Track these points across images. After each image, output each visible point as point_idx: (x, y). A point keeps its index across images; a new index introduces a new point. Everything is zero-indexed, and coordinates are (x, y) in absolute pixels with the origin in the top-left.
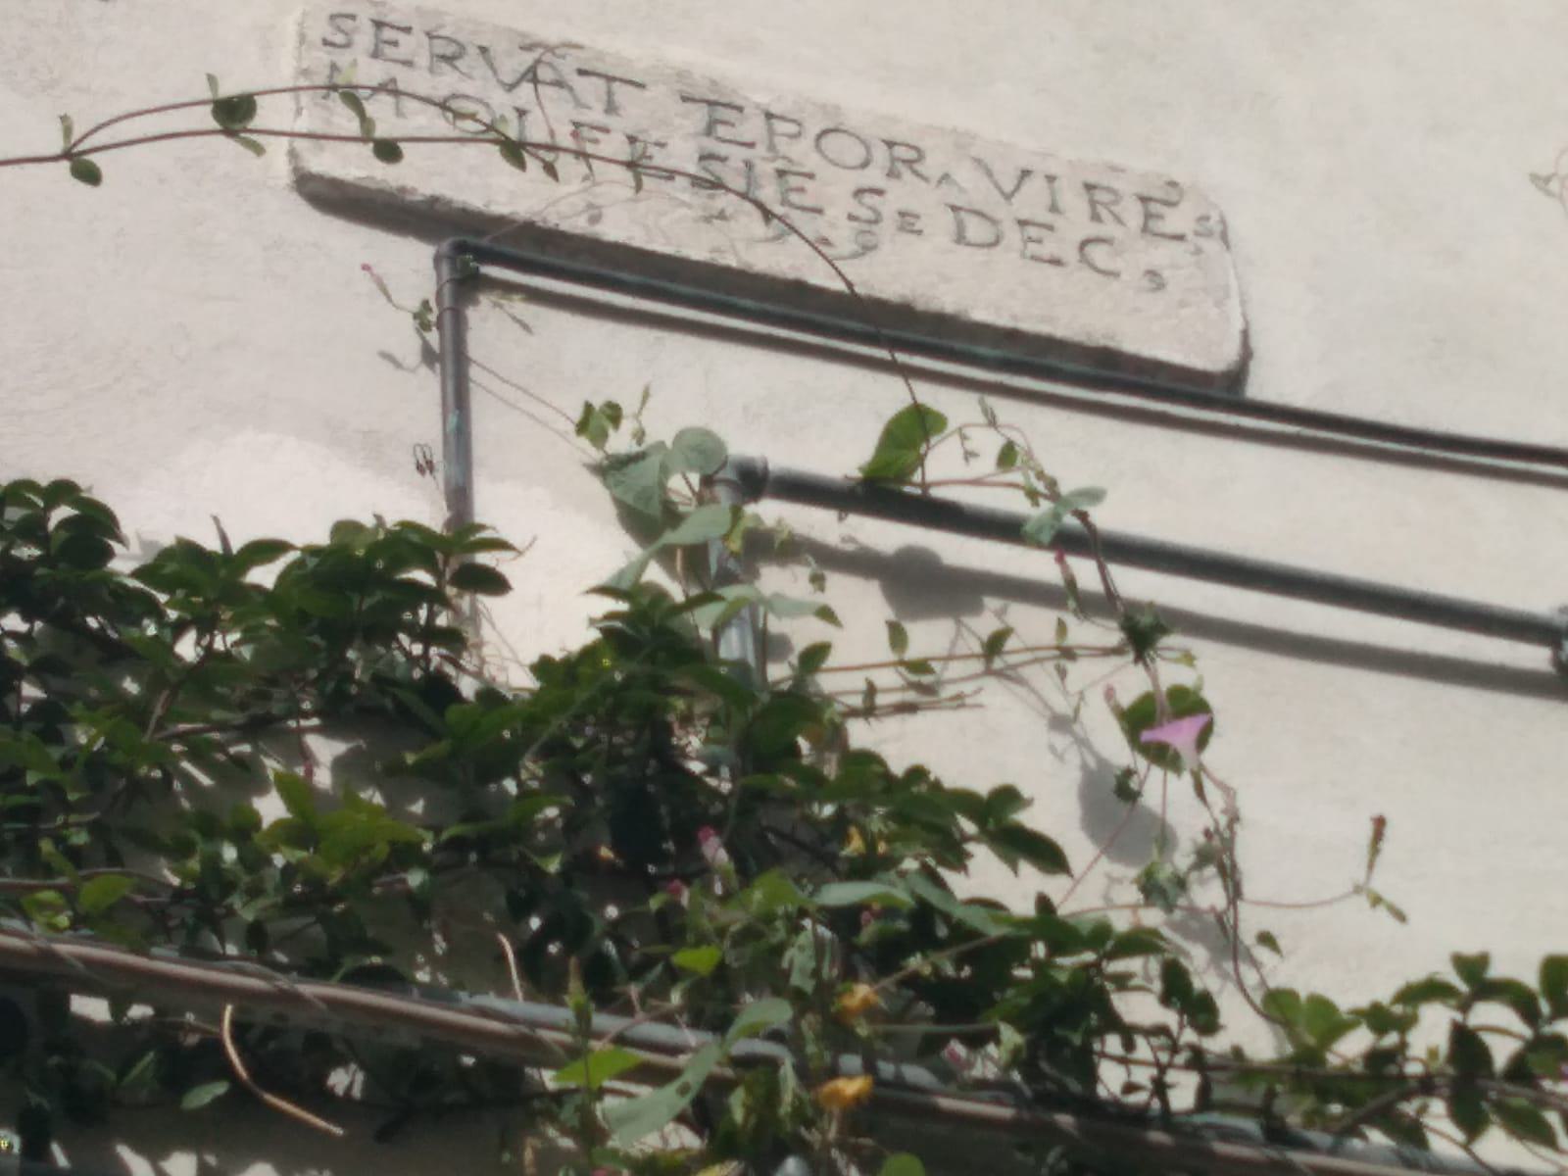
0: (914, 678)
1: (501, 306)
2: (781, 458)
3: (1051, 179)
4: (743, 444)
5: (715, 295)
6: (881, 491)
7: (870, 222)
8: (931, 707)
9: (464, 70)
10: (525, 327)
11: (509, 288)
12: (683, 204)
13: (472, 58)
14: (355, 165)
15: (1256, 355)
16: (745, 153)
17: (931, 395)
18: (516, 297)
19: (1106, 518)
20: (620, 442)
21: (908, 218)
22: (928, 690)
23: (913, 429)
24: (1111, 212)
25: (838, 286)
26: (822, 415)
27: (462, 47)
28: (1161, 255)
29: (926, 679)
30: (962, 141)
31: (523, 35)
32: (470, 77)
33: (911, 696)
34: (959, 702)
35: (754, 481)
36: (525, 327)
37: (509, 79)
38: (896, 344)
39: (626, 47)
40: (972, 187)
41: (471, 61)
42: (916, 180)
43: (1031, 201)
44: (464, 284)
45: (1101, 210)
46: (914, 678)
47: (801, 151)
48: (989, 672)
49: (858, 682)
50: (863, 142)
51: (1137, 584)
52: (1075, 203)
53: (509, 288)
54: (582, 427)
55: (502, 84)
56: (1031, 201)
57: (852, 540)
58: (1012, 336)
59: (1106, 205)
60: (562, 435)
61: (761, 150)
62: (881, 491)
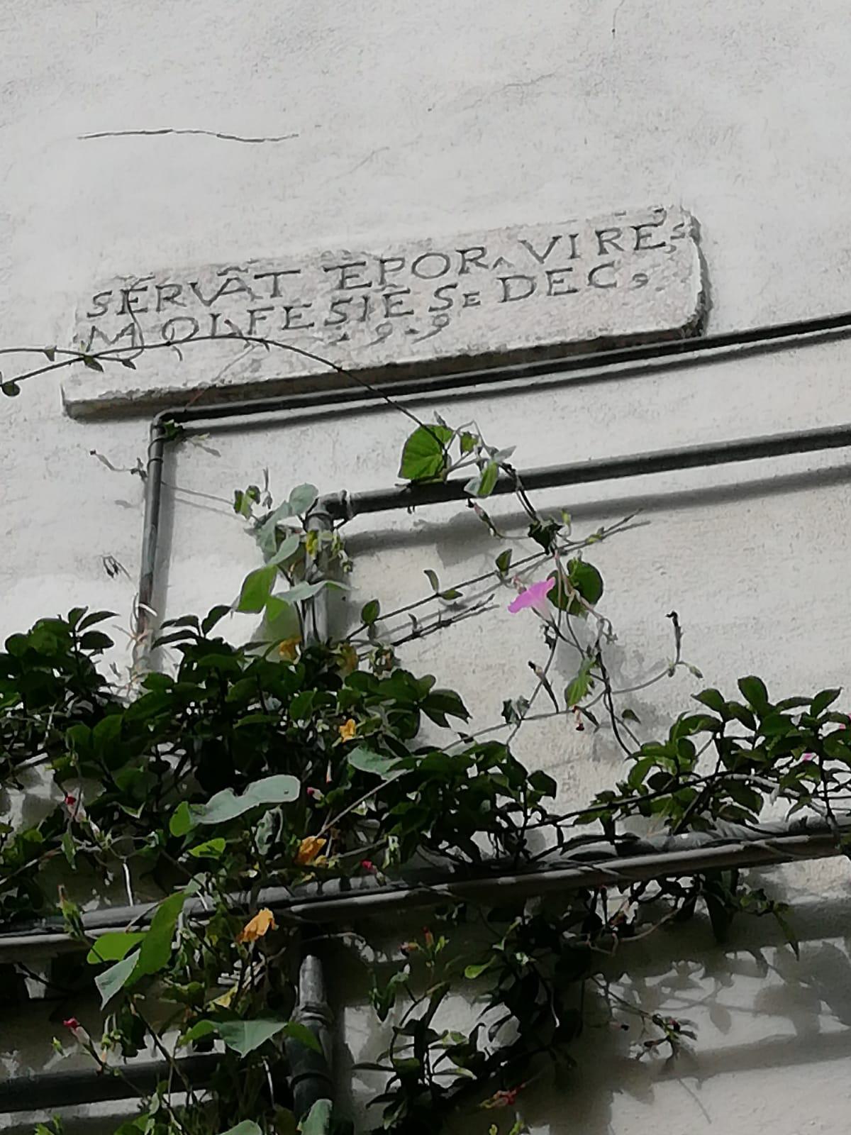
0: (451, 602)
1: (200, 445)
2: (356, 487)
3: (193, 285)
4: (327, 489)
5: (431, 380)
6: (427, 487)
7: (444, 308)
8: (459, 618)
9: (180, 301)
10: (215, 453)
11: (201, 431)
12: (316, 339)
13: (187, 295)
14: (94, 388)
15: (716, 306)
16: (364, 291)
17: (426, 416)
18: (205, 436)
19: (522, 463)
20: (259, 511)
21: (470, 297)
22: (455, 607)
23: (428, 443)
24: (615, 245)
25: (327, 369)
26: (363, 453)
27: (180, 287)
28: (644, 262)
29: (458, 600)
30: (510, 233)
31: (220, 266)
32: (184, 305)
33: (449, 615)
34: (479, 609)
35: (339, 509)
36: (215, 453)
37: (207, 298)
38: (386, 393)
39: (273, 252)
40: (518, 259)
41: (187, 295)
42: (479, 269)
43: (558, 257)
44: (170, 438)
45: (606, 245)
46: (451, 602)
47: (404, 278)
48: (504, 582)
49: (404, 618)
50: (445, 257)
51: (543, 499)
52: (588, 247)
53: (201, 431)
54: (237, 507)
55: (203, 301)
56: (558, 257)
57: (421, 522)
58: (538, 351)
59: (608, 241)
60: (230, 515)
61: (375, 286)
62: (427, 487)
